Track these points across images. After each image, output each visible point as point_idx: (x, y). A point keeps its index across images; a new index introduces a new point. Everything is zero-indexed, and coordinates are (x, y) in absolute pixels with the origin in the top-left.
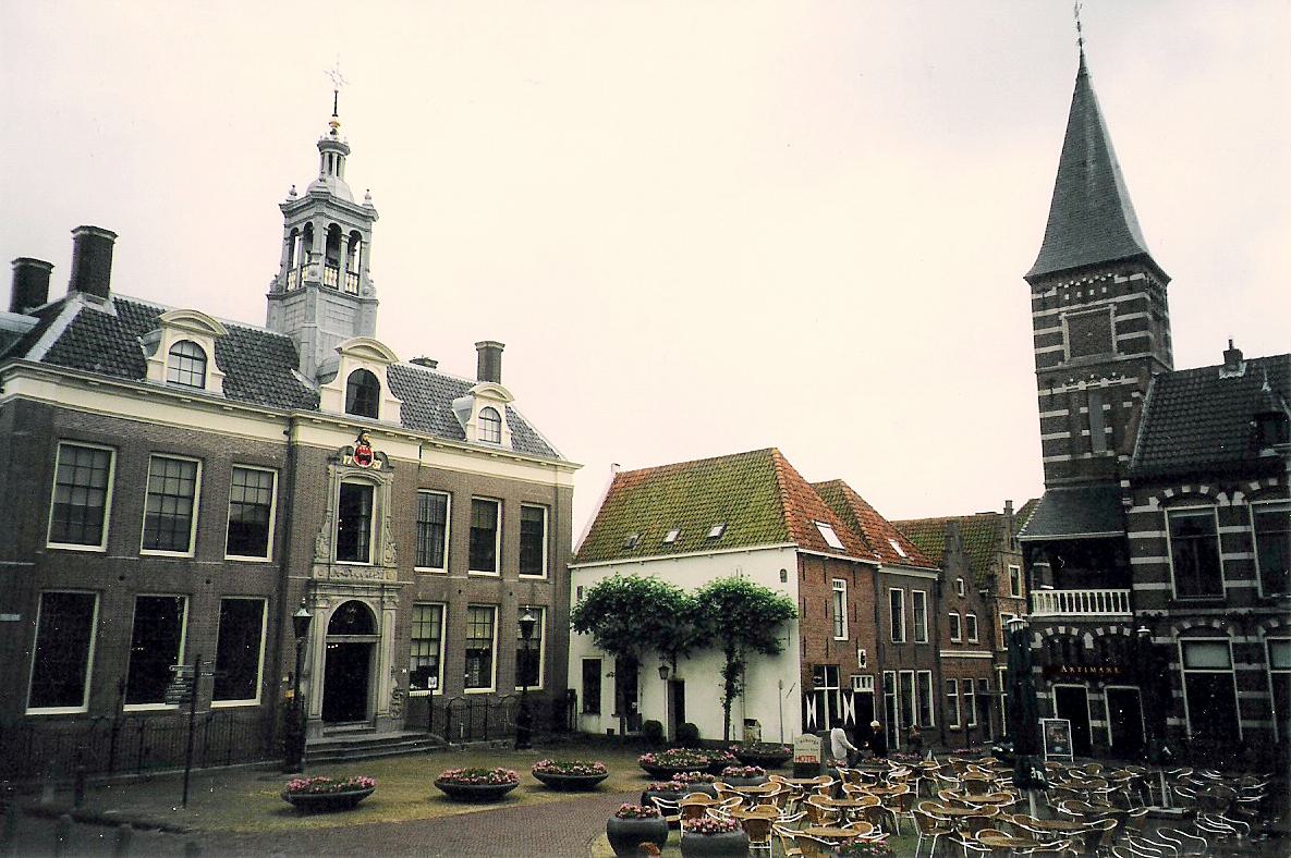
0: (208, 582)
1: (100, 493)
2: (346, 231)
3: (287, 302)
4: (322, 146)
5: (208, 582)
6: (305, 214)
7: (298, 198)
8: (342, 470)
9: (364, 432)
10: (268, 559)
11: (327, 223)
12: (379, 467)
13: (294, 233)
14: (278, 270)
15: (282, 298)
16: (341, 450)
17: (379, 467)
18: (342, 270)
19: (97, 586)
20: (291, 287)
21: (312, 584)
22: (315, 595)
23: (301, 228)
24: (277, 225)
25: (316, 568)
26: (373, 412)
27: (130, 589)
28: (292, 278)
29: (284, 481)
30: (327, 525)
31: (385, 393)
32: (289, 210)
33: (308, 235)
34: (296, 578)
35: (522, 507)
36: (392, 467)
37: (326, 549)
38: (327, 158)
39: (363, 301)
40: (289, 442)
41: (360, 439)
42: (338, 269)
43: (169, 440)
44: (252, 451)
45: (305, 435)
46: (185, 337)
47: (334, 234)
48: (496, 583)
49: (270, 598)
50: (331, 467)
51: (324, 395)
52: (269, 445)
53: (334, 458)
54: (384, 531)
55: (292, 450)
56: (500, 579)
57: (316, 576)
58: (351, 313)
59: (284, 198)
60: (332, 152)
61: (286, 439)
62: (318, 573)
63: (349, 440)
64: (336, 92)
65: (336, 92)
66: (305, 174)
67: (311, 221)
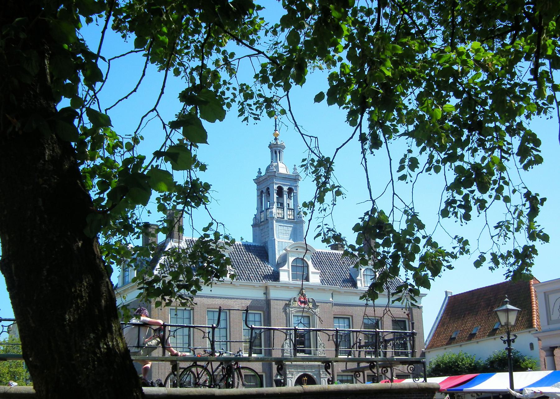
2: (285, 188)
4: (270, 146)
7: (262, 175)
11: (275, 187)
13: (262, 192)
14: (255, 212)
18: (285, 208)
20: (262, 220)
23: (265, 191)
24: (253, 190)
26: (307, 279)
28: (262, 216)
31: (312, 268)
32: (259, 181)
33: (268, 193)
38: (274, 152)
42: (284, 208)
47: (280, 191)
51: (282, 274)
59: (255, 175)
63: (294, 294)
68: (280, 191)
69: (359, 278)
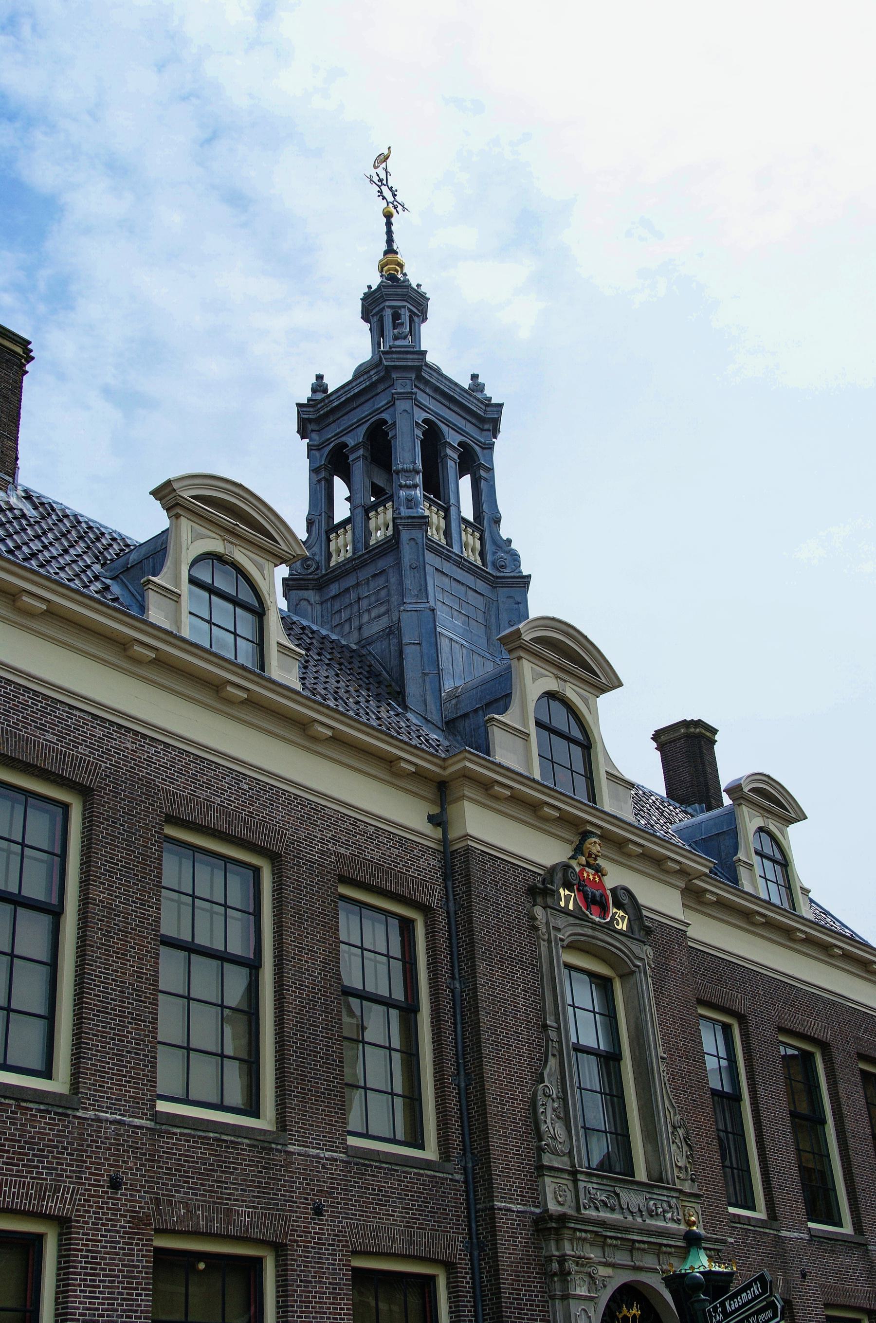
0: (318, 1211)
1: (45, 920)
2: (453, 438)
3: (334, 589)
5: (318, 1211)
6: (366, 410)
8: (561, 921)
9: (585, 835)
10: (430, 1153)
11: (420, 416)
12: (623, 926)
15: (320, 585)
16: (552, 871)
17: (623, 926)
19: (52, 1206)
21: (547, 1226)
22: (562, 1259)
25: (549, 1184)
27: (139, 1222)
29: (442, 941)
30: (552, 1062)
33: (380, 444)
34: (510, 1206)
35: (360, 1276)
36: (648, 931)
37: (559, 1130)
39: (504, 578)
40: (445, 841)
41: (579, 850)
43: (203, 794)
44: (373, 854)
45: (482, 825)
46: (216, 545)
48: (850, 1260)
49: (449, 1267)
50: (539, 911)
52: (401, 842)
53: (540, 887)
54: (663, 1102)
55: (458, 862)
56: (857, 1245)
57: (553, 1207)
58: (479, 601)
60: (394, 305)
61: (438, 833)
62: (555, 1197)
64: (388, 216)
65: (388, 216)
66: (345, 351)
67: (384, 416)
68: (432, 439)
69: (741, 855)
